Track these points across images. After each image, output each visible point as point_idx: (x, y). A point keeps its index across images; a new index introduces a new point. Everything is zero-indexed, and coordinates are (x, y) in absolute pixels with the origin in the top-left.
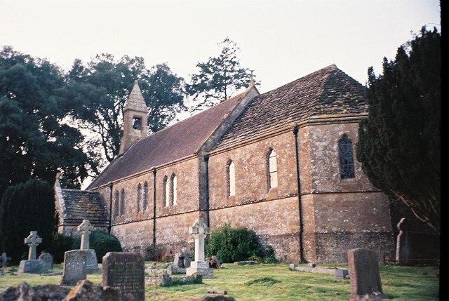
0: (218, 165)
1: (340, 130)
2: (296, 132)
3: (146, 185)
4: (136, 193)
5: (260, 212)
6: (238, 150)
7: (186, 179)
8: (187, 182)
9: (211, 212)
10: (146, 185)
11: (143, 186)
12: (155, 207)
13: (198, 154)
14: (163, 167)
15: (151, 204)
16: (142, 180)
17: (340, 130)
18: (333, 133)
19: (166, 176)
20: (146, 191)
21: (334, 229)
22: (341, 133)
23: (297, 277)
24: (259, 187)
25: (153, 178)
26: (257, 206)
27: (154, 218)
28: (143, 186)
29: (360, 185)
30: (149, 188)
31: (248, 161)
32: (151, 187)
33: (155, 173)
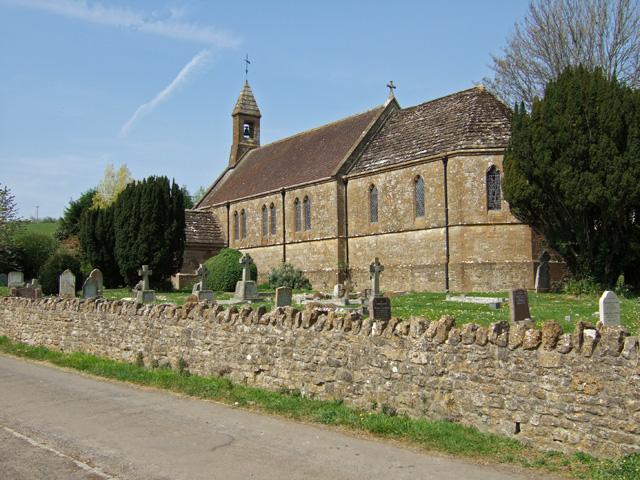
0: (358, 190)
1: (489, 161)
2: (445, 161)
3: (272, 206)
4: (260, 215)
5: (405, 241)
6: (382, 175)
7: (323, 203)
8: (324, 207)
9: (350, 240)
10: (272, 206)
11: (268, 207)
12: (284, 232)
13: (336, 177)
14: (294, 188)
15: (280, 228)
16: (267, 200)
17: (489, 161)
18: (480, 165)
19: (297, 199)
20: (273, 213)
21: (480, 260)
22: (490, 164)
23: (246, 285)
24: (405, 215)
25: (281, 199)
26: (402, 236)
27: (284, 244)
28: (268, 207)
29: (504, 217)
30: (278, 210)
31: (394, 188)
32: (279, 210)
33: (284, 195)
